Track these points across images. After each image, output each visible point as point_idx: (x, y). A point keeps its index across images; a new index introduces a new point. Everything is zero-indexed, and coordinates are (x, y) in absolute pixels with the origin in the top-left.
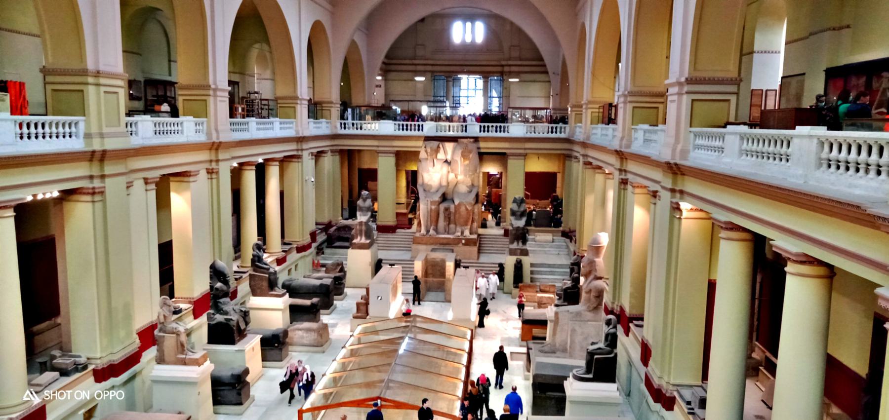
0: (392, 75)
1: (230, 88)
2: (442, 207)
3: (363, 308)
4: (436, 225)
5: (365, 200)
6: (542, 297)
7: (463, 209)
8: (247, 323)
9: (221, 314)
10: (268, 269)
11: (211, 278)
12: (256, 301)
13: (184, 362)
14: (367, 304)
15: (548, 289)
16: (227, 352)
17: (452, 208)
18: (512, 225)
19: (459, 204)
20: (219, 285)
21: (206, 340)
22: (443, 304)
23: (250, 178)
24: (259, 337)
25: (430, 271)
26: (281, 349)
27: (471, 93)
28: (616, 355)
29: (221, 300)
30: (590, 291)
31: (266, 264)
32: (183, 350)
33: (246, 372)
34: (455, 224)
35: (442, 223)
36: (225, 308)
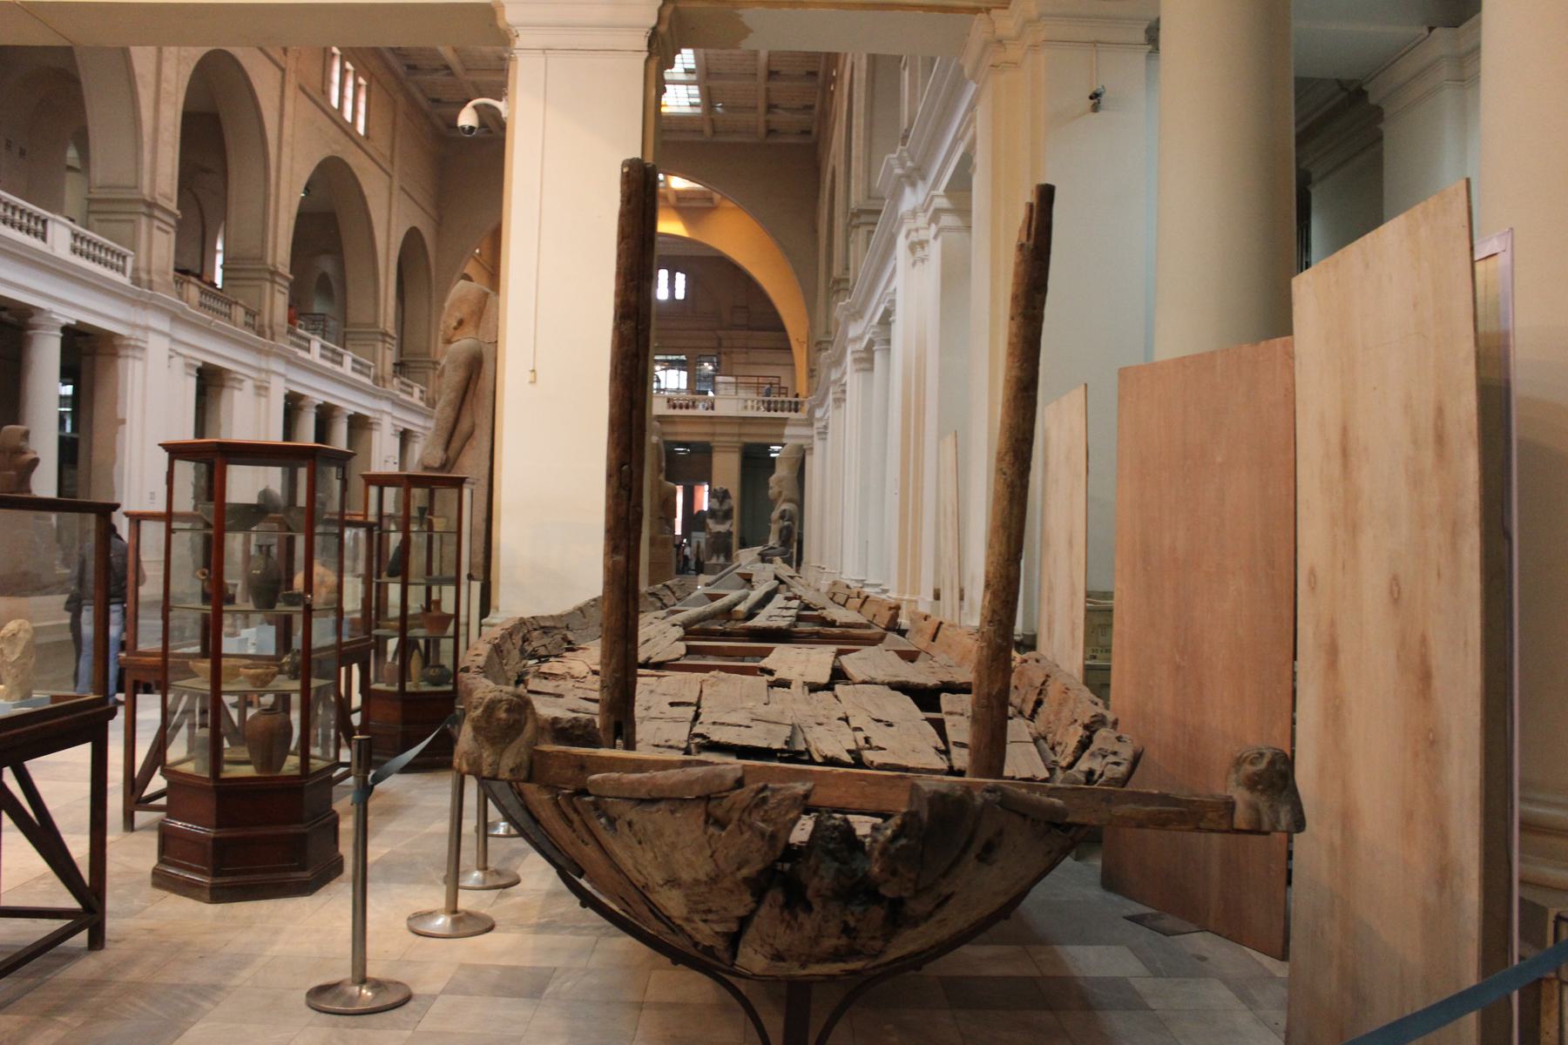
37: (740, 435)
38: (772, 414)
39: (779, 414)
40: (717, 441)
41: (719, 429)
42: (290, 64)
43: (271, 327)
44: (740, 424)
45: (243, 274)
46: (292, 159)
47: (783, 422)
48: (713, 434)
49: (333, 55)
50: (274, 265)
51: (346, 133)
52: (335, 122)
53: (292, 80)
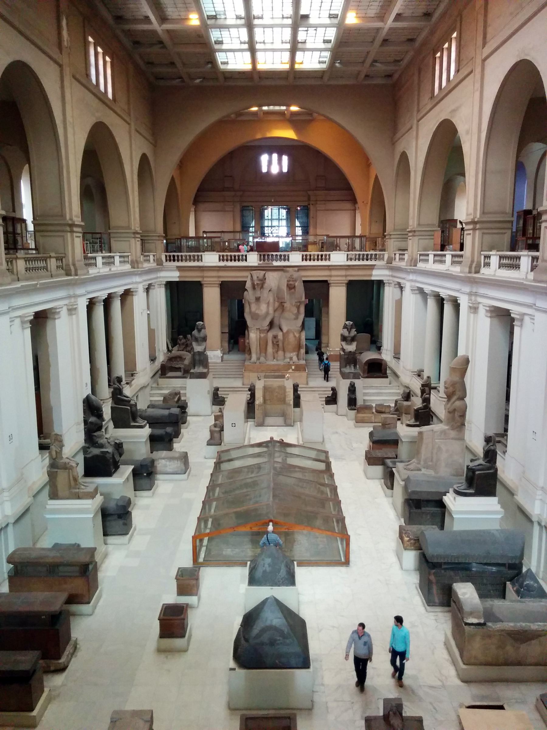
0: (202, 206)
1: (83, 224)
2: (270, 335)
3: (216, 435)
4: (266, 353)
5: (199, 331)
6: (385, 418)
7: (291, 336)
8: (121, 455)
9: (96, 447)
10: (129, 401)
11: (85, 412)
12: (123, 434)
13: (78, 497)
14: (222, 429)
15: (383, 410)
16: (106, 485)
17: (280, 335)
18: (343, 350)
19: (288, 332)
20: (92, 419)
21: (83, 473)
22: (286, 429)
23: (99, 311)
24: (133, 467)
25: (267, 398)
26: (150, 479)
27: (275, 223)
28: (496, 470)
29: (95, 434)
30: (455, 410)
31: (128, 397)
32: (76, 484)
33: (129, 502)
34: (284, 351)
35: (270, 349)
36: (101, 441)
37: (346, 276)
38: (365, 263)
39: (369, 263)
40: (331, 280)
41: (334, 273)
42: (64, 60)
43: (74, 265)
44: (346, 269)
45: (50, 228)
46: (74, 134)
47: (372, 267)
48: (331, 276)
49: (90, 42)
50: (71, 219)
51: (100, 99)
52: (94, 94)
53: (67, 71)
